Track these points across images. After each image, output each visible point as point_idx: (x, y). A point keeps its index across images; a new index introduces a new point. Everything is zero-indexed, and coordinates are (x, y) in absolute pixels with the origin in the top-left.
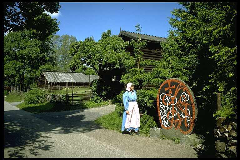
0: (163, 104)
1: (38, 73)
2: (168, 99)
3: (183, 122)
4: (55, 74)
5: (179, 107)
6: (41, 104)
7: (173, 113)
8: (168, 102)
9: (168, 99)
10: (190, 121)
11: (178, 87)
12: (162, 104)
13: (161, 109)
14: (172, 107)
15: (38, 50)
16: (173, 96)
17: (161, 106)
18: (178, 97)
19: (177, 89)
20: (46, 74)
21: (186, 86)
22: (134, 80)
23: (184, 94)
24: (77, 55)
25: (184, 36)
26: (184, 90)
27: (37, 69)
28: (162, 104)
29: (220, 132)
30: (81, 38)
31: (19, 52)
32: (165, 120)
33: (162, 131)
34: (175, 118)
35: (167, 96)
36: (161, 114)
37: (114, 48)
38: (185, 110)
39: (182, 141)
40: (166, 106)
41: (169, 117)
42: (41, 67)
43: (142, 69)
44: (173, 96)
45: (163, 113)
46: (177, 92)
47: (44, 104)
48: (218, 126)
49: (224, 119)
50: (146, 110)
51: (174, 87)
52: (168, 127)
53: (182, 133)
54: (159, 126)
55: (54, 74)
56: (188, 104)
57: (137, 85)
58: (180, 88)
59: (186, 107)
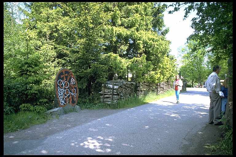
3: (73, 98)
18: (69, 81)
23: (72, 80)
26: (72, 77)
51: (67, 75)
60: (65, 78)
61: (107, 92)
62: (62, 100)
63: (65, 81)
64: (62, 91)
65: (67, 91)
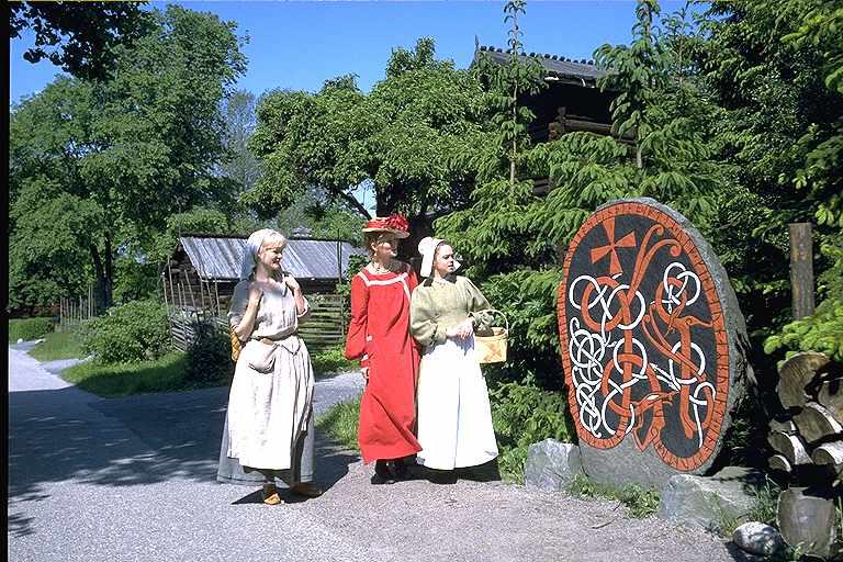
0: (584, 326)
1: (163, 244)
2: (603, 301)
3: (672, 409)
4: (230, 246)
5: (656, 336)
6: (151, 364)
8: (607, 313)
9: (603, 301)
10: (705, 403)
11: (644, 245)
12: (578, 325)
13: (575, 349)
14: (622, 341)
15: (159, 149)
16: (628, 287)
17: (574, 338)
18: (650, 287)
19: (642, 250)
20: (192, 246)
21: (685, 231)
22: (484, 234)
23: (676, 271)
24: (281, 152)
25: (739, 33)
26: (675, 251)
27: (161, 226)
28: (578, 325)
29: (803, 440)
30: (310, 84)
31: (88, 158)
32: (592, 404)
33: (577, 460)
34: (640, 391)
35: (598, 289)
36: (577, 373)
37: (435, 118)
38: (679, 350)
39: (664, 505)
40: (596, 336)
41: (611, 388)
42: (174, 221)
43: (528, 187)
44: (628, 287)
45: (585, 370)
46: (642, 265)
47: (164, 362)
48: (787, 402)
49: (816, 361)
50: (530, 366)
51: (630, 240)
52: (606, 435)
53: (669, 464)
54: (575, 440)
55: (224, 245)
56: (696, 321)
57: (503, 255)
58: (659, 245)
59: (686, 336)
63: (620, 281)
64: (597, 346)
65: (628, 349)
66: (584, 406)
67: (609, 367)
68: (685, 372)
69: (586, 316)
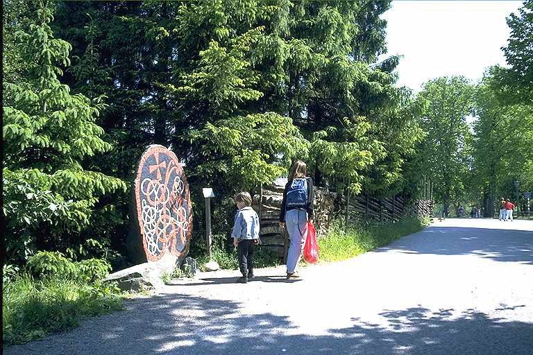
7: (165, 220)
8: (157, 197)
11: (169, 167)
12: (145, 203)
17: (144, 211)
19: (168, 171)
36: (146, 227)
46: (168, 175)
58: (173, 168)
60: (159, 176)
61: (268, 219)
62: (152, 239)
65: (165, 212)
66: (149, 244)
67: (158, 221)
68: (181, 220)
69: (148, 198)
